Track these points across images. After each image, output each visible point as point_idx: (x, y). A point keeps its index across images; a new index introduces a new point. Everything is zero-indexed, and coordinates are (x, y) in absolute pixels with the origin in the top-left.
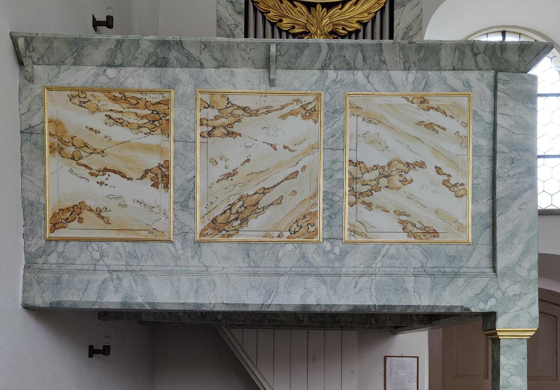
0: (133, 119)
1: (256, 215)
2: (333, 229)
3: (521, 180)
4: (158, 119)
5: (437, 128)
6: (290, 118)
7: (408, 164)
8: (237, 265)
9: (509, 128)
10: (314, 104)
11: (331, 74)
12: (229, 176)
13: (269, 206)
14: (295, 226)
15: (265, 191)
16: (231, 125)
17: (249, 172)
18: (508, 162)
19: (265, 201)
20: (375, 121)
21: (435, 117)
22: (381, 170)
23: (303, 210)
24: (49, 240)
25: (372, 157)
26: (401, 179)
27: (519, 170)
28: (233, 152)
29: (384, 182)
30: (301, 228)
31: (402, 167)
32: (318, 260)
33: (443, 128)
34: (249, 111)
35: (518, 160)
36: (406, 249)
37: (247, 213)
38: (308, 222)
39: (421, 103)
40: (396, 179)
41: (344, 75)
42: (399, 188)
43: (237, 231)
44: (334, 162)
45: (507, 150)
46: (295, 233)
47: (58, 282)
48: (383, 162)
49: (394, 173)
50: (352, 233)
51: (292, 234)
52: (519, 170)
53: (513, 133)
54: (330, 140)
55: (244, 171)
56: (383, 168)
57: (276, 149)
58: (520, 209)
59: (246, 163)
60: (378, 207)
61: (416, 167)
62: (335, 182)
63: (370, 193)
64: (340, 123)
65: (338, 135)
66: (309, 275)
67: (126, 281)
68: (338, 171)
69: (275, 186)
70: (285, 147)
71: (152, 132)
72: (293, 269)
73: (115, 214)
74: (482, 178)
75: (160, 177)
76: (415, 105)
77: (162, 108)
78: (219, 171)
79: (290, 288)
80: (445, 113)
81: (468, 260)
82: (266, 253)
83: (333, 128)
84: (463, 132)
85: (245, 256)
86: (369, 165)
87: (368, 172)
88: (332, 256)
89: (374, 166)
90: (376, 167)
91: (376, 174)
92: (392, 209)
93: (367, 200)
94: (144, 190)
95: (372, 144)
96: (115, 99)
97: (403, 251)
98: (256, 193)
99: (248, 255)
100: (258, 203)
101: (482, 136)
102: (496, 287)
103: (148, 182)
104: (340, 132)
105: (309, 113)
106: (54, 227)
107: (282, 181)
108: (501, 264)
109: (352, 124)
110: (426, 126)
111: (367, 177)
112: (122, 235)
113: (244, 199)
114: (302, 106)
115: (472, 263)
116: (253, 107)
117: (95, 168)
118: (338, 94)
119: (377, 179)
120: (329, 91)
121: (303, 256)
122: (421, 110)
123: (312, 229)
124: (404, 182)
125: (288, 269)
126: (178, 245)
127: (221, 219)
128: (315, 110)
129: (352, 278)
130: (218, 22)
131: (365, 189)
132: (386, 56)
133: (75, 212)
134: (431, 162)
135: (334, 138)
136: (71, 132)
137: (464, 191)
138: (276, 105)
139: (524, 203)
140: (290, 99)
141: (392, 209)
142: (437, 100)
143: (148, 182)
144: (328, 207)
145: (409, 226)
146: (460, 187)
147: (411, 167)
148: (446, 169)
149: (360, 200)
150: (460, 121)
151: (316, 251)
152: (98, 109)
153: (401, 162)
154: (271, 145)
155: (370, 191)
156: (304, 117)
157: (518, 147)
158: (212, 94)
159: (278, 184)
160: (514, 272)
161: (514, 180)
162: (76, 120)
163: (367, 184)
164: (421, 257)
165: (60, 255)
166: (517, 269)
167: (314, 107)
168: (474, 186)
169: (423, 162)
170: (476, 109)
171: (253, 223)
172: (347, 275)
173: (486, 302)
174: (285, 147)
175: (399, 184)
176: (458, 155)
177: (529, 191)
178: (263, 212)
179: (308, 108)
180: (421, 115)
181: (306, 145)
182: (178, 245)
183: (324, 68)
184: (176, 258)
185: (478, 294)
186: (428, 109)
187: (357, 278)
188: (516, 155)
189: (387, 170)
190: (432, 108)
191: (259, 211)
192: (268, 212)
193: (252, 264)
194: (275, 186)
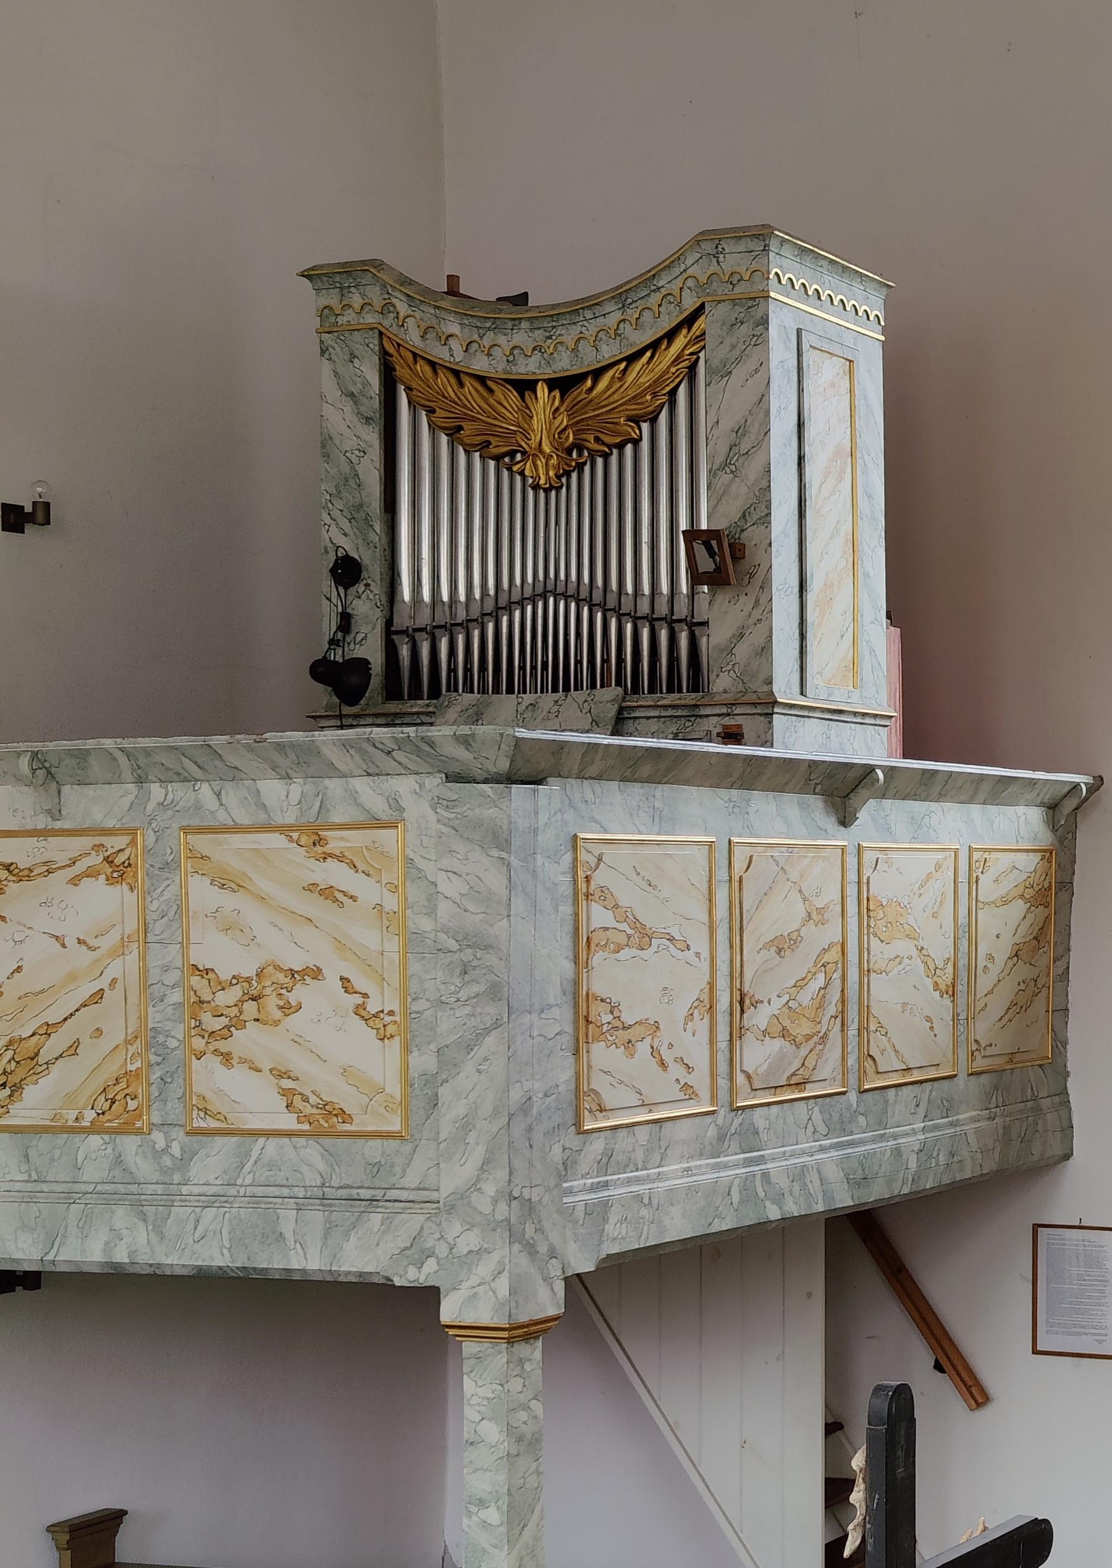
1: (35, 1077)
2: (169, 1104)
3: (479, 1010)
5: (340, 896)
6: (86, 882)
7: (292, 973)
8: (8, 1178)
9: (458, 901)
13: (56, 1059)
14: (102, 1098)
15: (48, 1030)
17: (21, 993)
18: (458, 971)
21: (335, 874)
22: (246, 985)
23: (113, 1069)
25: (229, 958)
26: (281, 1003)
27: (476, 988)
29: (250, 1007)
30: (113, 1102)
31: (281, 978)
32: (144, 1168)
33: (351, 897)
34: (17, 871)
36: (295, 1147)
38: (126, 1091)
39: (314, 844)
40: (272, 1003)
41: (178, 791)
42: (277, 1023)
45: (455, 946)
46: (103, 1113)
48: (250, 971)
49: (268, 991)
50: (202, 1114)
51: (98, 1114)
52: (476, 988)
56: (248, 980)
58: (479, 1071)
59: (16, 974)
60: (243, 1061)
61: (306, 977)
62: (170, 1010)
63: (226, 1033)
64: (174, 888)
65: (171, 913)
68: (173, 987)
69: (65, 1019)
70: (80, 941)
72: (99, 1188)
74: (427, 1000)
79: (86, 1227)
81: (404, 1172)
82: (57, 1153)
83: (162, 899)
84: (391, 903)
85: (22, 1159)
86: (225, 975)
87: (223, 989)
88: (167, 1161)
89: (234, 977)
91: (236, 993)
92: (266, 1066)
93: (223, 1046)
97: (290, 1152)
98: (33, 1034)
99: (27, 1157)
100: (37, 1054)
102: (437, 1236)
104: (175, 908)
105: (118, 871)
107: (77, 1010)
110: (321, 892)
111: (224, 999)
113: (16, 1045)
118: (168, 831)
120: (154, 825)
121: (118, 1160)
123: (132, 1105)
124: (287, 1009)
125: (91, 1188)
129: (190, 1210)
130: (323, 446)
131: (218, 1024)
134: (334, 968)
137: (395, 1027)
138: (61, 859)
139: (486, 1059)
140: (87, 842)
141: (266, 1066)
142: (342, 839)
144: (159, 1059)
145: (297, 1100)
146: (388, 1019)
147: (298, 978)
148: (359, 983)
149: (212, 1048)
150: (384, 881)
151: (140, 1150)
153: (281, 969)
154: (57, 938)
155: (228, 1027)
159: (71, 1015)
160: (469, 1203)
161: (467, 1010)
163: (222, 1015)
164: (321, 1166)
166: (475, 1197)
168: (413, 1016)
169: (318, 968)
170: (412, 856)
171: (32, 1093)
173: (420, 1266)
174: (80, 941)
175: (278, 1014)
177: (493, 1033)
178: (46, 1072)
179: (118, 861)
181: (113, 938)
185: (406, 1248)
187: (198, 1210)
188: (472, 957)
189: (255, 984)
190: (331, 855)
191: (40, 1069)
192: (55, 1070)
193: (34, 1176)
194: (65, 1019)
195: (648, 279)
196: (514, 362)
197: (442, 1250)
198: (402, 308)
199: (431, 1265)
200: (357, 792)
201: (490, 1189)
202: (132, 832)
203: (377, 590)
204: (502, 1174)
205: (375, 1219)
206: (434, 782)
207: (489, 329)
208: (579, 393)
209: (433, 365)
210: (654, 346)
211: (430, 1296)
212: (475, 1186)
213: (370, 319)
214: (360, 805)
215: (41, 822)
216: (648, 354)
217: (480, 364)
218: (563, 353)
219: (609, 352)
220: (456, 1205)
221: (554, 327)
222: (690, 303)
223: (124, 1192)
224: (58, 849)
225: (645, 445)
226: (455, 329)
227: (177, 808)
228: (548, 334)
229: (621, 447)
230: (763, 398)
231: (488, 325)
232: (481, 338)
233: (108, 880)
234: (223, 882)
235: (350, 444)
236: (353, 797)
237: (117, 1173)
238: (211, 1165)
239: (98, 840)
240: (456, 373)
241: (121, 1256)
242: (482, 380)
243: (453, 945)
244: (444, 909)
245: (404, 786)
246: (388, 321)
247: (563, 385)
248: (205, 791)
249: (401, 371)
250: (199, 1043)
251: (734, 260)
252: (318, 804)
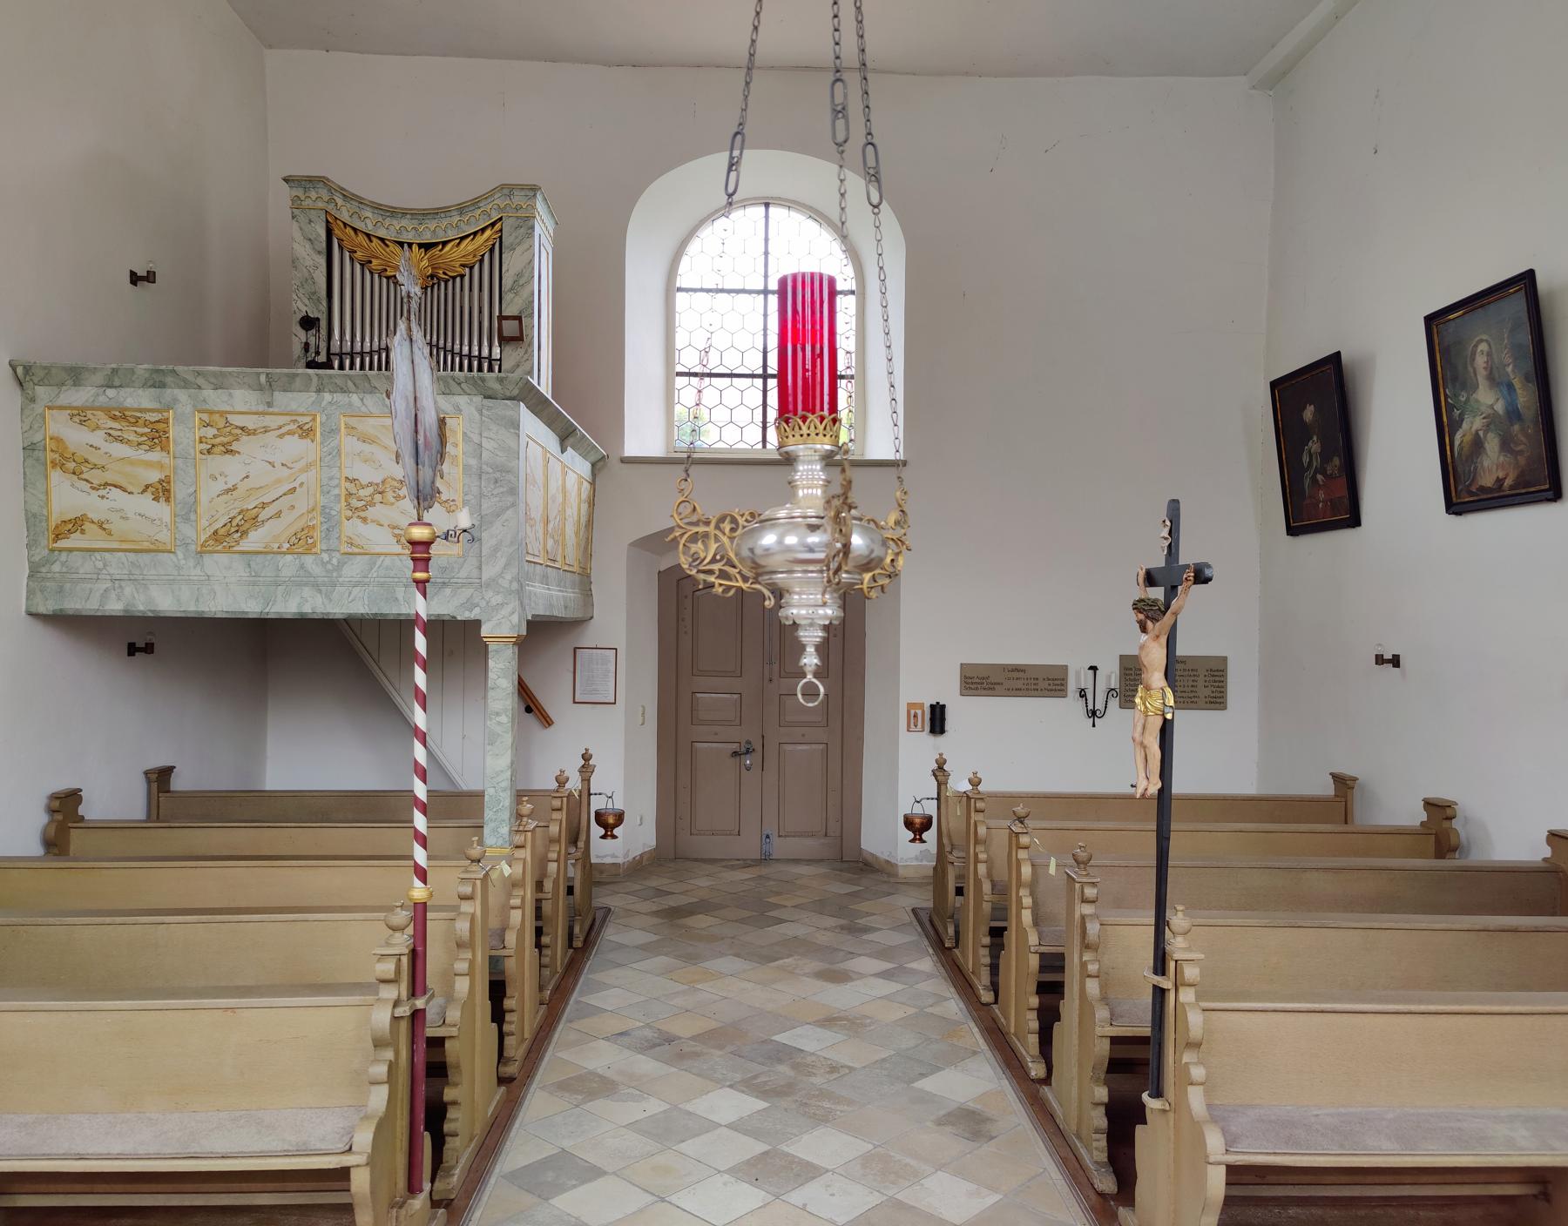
0: (132, 437)
4: (157, 437)
11: (327, 397)
12: (228, 491)
15: (264, 506)
16: (230, 443)
19: (264, 515)
24: (52, 550)
25: (366, 474)
28: (232, 469)
29: (378, 497)
37: (247, 526)
40: (390, 496)
41: (338, 397)
43: (237, 542)
44: (331, 478)
47: (61, 590)
55: (242, 487)
66: (306, 584)
67: (128, 590)
71: (151, 448)
73: (116, 526)
75: (162, 491)
77: (161, 426)
78: (220, 486)
90: (371, 484)
91: (370, 490)
93: (362, 514)
94: (146, 503)
96: (114, 418)
103: (149, 496)
105: (306, 432)
106: (57, 537)
108: (485, 577)
109: (349, 444)
111: (362, 493)
112: (124, 546)
115: (463, 574)
116: (251, 426)
117: (96, 482)
119: (372, 496)
121: (302, 567)
126: (180, 556)
127: (222, 532)
132: (375, 383)
133: (77, 524)
136: (72, 449)
140: (288, 418)
143: (149, 496)
152: (98, 428)
156: (301, 437)
158: (211, 413)
162: (77, 437)
165: (63, 564)
171: (253, 535)
172: (342, 585)
181: (302, 463)
182: (180, 556)
183: (319, 391)
184: (179, 568)
192: (267, 525)
195: (475, 203)
197: (483, 604)
198: (340, 202)
199: (477, 610)
201: (508, 577)
203: (324, 332)
204: (515, 571)
205: (448, 591)
206: (478, 399)
208: (435, 251)
209: (355, 230)
210: (475, 234)
211: (477, 624)
212: (501, 575)
213: (320, 204)
215: (261, 408)
217: (382, 233)
219: (451, 234)
220: (492, 584)
223: (304, 580)
224: (270, 421)
225: (467, 278)
229: (454, 278)
230: (531, 261)
235: (309, 262)
237: (302, 573)
238: (354, 569)
240: (368, 236)
241: (307, 609)
242: (382, 240)
245: (462, 400)
246: (330, 208)
247: (426, 247)
248: (355, 398)
249: (336, 231)
250: (349, 513)
251: (518, 199)
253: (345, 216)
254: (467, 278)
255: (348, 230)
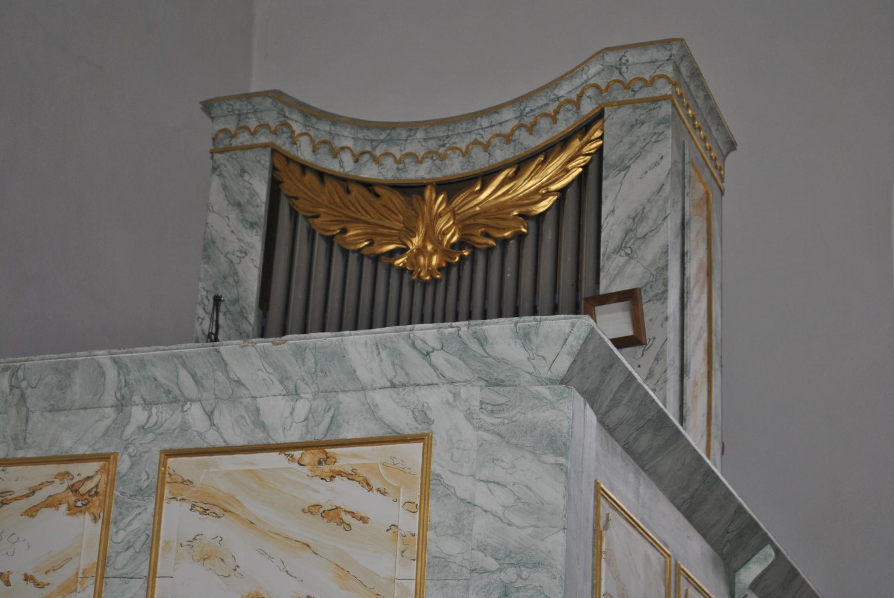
6: (45, 513)
9: (500, 514)
10: (96, 480)
20: (217, 510)
21: (346, 495)
33: (361, 518)
35: (518, 589)
39: (320, 463)
45: (493, 564)
53: (509, 525)
54: (121, 556)
57: (8, 583)
76: (305, 470)
80: (368, 484)
95: (207, 562)
101: (450, 532)
105: (81, 500)
109: (177, 518)
110: (325, 514)
114: (73, 485)
118: (147, 456)
120: (130, 450)
122: (317, 479)
128: (97, 493)
135: (130, 552)
138: (19, 488)
142: (354, 456)
150: (402, 500)
157: (519, 557)
167: (97, 486)
176: (393, 580)
179: (83, 489)
180: (316, 491)
186: (332, 477)
188: (515, 577)
190: (340, 474)
196: (405, 170)
200: (376, 406)
202: (104, 457)
207: (382, 141)
214: (379, 419)
216: (541, 158)
217: (370, 172)
218: (455, 160)
221: (448, 136)
222: (588, 108)
225: (529, 243)
226: (349, 143)
227: (158, 432)
228: (441, 143)
231: (382, 137)
232: (374, 148)
233: (69, 509)
234: (205, 506)
236: (372, 411)
239: (63, 468)
243: (493, 564)
244: (481, 527)
247: (452, 187)
252: (328, 420)
253: (304, 153)
254: (529, 243)
255: (310, 178)
